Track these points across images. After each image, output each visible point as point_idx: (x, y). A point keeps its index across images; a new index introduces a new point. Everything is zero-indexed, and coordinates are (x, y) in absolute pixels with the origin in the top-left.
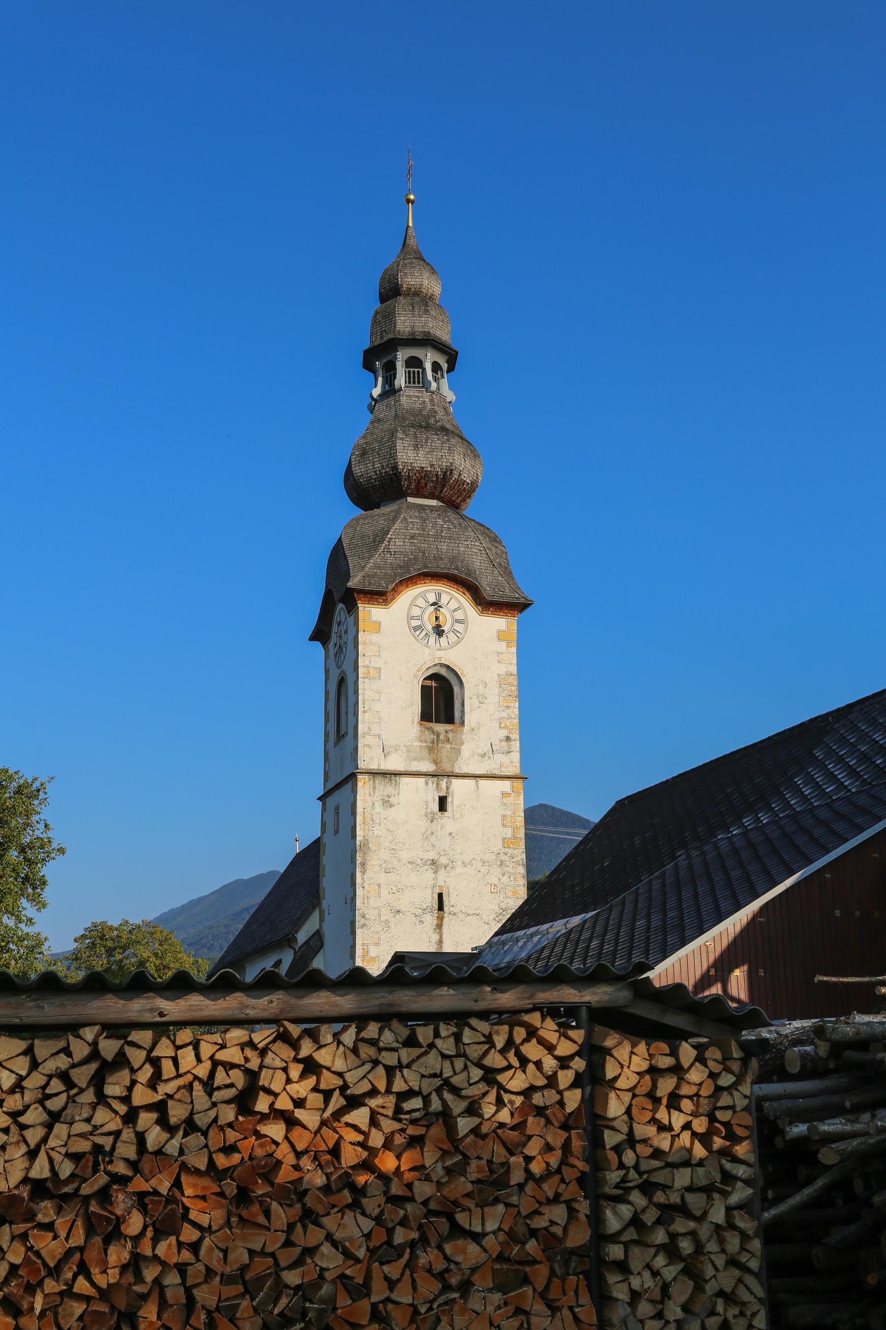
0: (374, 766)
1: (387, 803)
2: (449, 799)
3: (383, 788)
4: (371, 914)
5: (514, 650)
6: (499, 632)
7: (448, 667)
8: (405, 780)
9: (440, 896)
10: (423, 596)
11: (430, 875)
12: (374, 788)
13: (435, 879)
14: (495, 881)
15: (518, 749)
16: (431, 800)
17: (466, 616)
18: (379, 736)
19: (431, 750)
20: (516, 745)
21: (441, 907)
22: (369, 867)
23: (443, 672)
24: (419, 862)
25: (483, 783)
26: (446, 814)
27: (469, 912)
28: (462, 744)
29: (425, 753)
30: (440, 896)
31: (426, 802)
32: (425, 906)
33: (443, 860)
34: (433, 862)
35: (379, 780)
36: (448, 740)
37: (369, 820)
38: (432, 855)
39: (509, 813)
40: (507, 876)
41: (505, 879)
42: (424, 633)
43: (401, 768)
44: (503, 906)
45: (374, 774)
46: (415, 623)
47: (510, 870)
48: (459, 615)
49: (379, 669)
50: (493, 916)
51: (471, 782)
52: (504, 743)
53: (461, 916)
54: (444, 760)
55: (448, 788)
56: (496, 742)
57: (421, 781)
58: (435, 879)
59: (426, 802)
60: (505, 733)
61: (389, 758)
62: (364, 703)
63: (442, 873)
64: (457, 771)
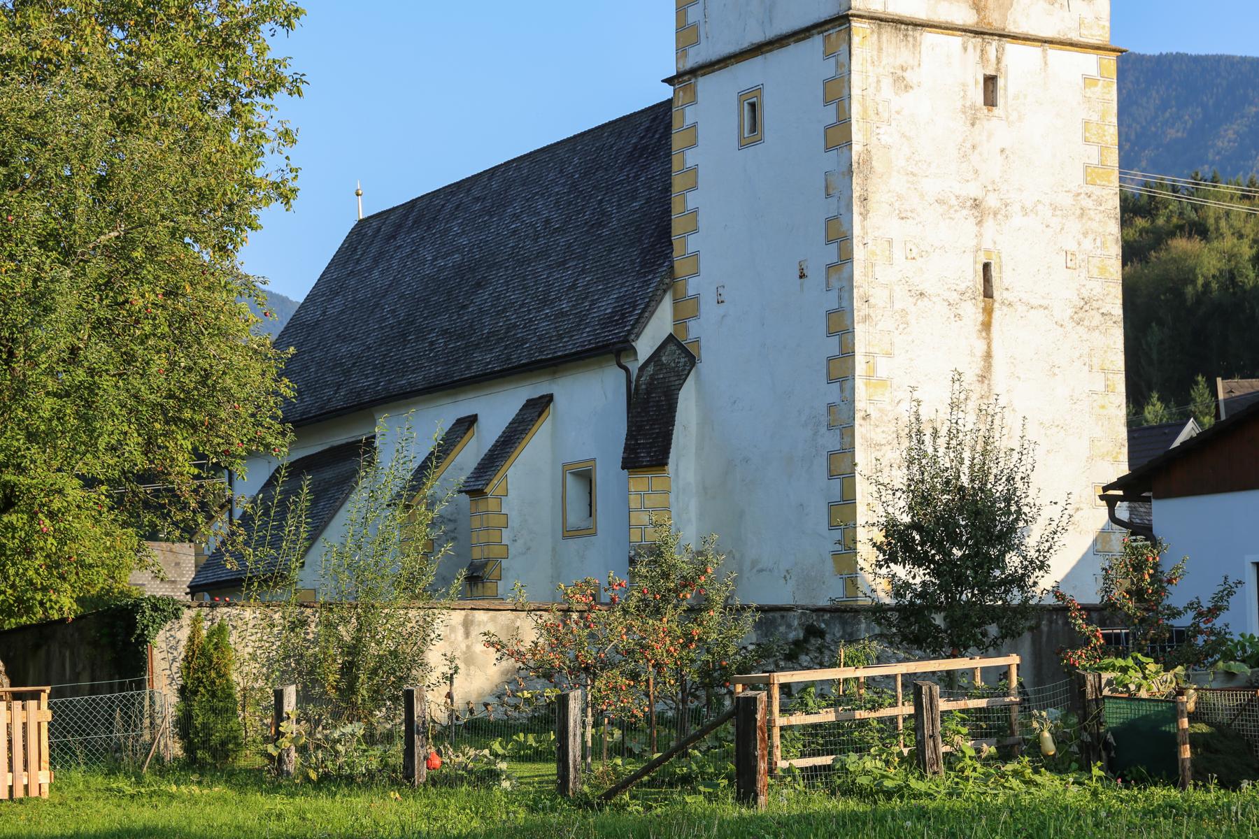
1: (901, 82)
2: (1001, 82)
4: (879, 297)
9: (986, 267)
11: (970, 226)
12: (880, 49)
13: (979, 235)
14: (1072, 246)
16: (971, 83)
21: (988, 294)
22: (872, 204)
24: (954, 202)
25: (1054, 53)
26: (996, 111)
27: (1034, 302)
30: (986, 267)
31: (964, 85)
32: (962, 287)
33: (992, 201)
34: (976, 204)
35: (888, 31)
37: (871, 113)
38: (973, 190)
39: (1095, 118)
40: (1091, 237)
41: (1087, 244)
43: (921, 15)
44: (1086, 295)
45: (880, 20)
47: (1095, 225)
50: (1070, 312)
51: (1034, 51)
53: (1021, 308)
55: (999, 60)
57: (956, 41)
58: (979, 235)
59: (964, 85)
63: (989, 223)
64: (1012, 28)
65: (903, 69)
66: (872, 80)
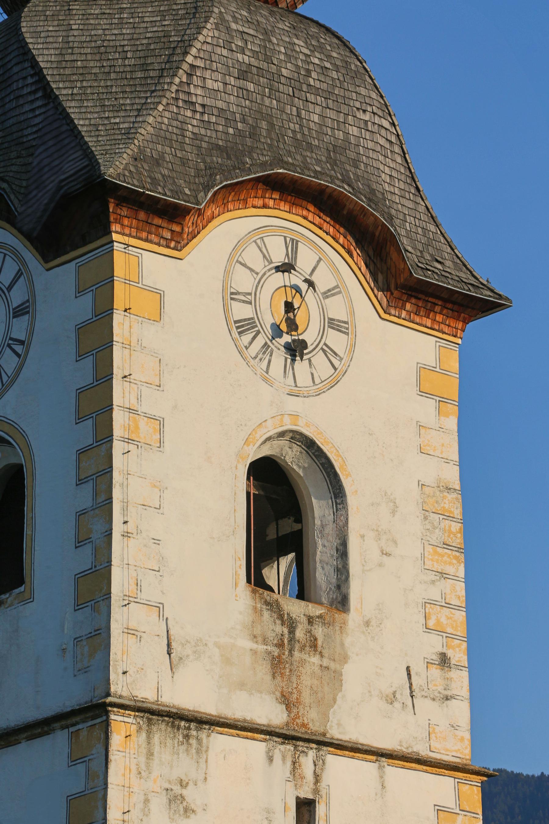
0: (146, 693)
2: (320, 810)
3: (170, 757)
5: (452, 423)
6: (422, 369)
7: (310, 446)
8: (220, 742)
10: (258, 237)
12: (150, 754)
15: (465, 692)
16: (279, 807)
17: (352, 313)
18: (160, 608)
19: (277, 665)
20: (460, 681)
23: (292, 457)
25: (395, 773)
28: (345, 659)
29: (263, 670)
35: (161, 731)
36: (314, 646)
42: (260, 341)
43: (209, 707)
45: (153, 714)
46: (242, 311)
48: (336, 309)
49: (161, 422)
51: (364, 769)
52: (435, 672)
54: (306, 697)
55: (317, 778)
56: (418, 668)
57: (257, 748)
60: (434, 644)
61: (181, 672)
62: (124, 510)
64: (335, 733)
65: (183, 784)
66: (137, 798)
